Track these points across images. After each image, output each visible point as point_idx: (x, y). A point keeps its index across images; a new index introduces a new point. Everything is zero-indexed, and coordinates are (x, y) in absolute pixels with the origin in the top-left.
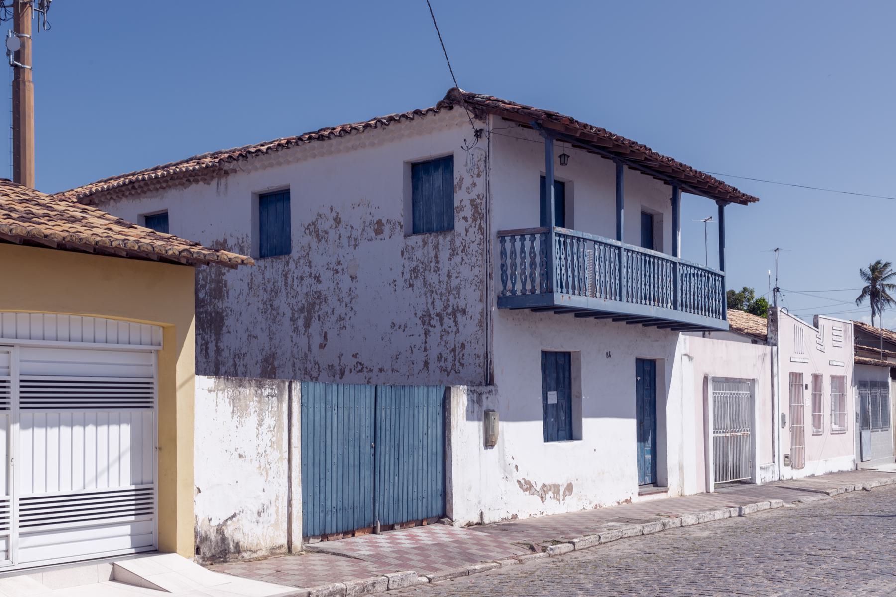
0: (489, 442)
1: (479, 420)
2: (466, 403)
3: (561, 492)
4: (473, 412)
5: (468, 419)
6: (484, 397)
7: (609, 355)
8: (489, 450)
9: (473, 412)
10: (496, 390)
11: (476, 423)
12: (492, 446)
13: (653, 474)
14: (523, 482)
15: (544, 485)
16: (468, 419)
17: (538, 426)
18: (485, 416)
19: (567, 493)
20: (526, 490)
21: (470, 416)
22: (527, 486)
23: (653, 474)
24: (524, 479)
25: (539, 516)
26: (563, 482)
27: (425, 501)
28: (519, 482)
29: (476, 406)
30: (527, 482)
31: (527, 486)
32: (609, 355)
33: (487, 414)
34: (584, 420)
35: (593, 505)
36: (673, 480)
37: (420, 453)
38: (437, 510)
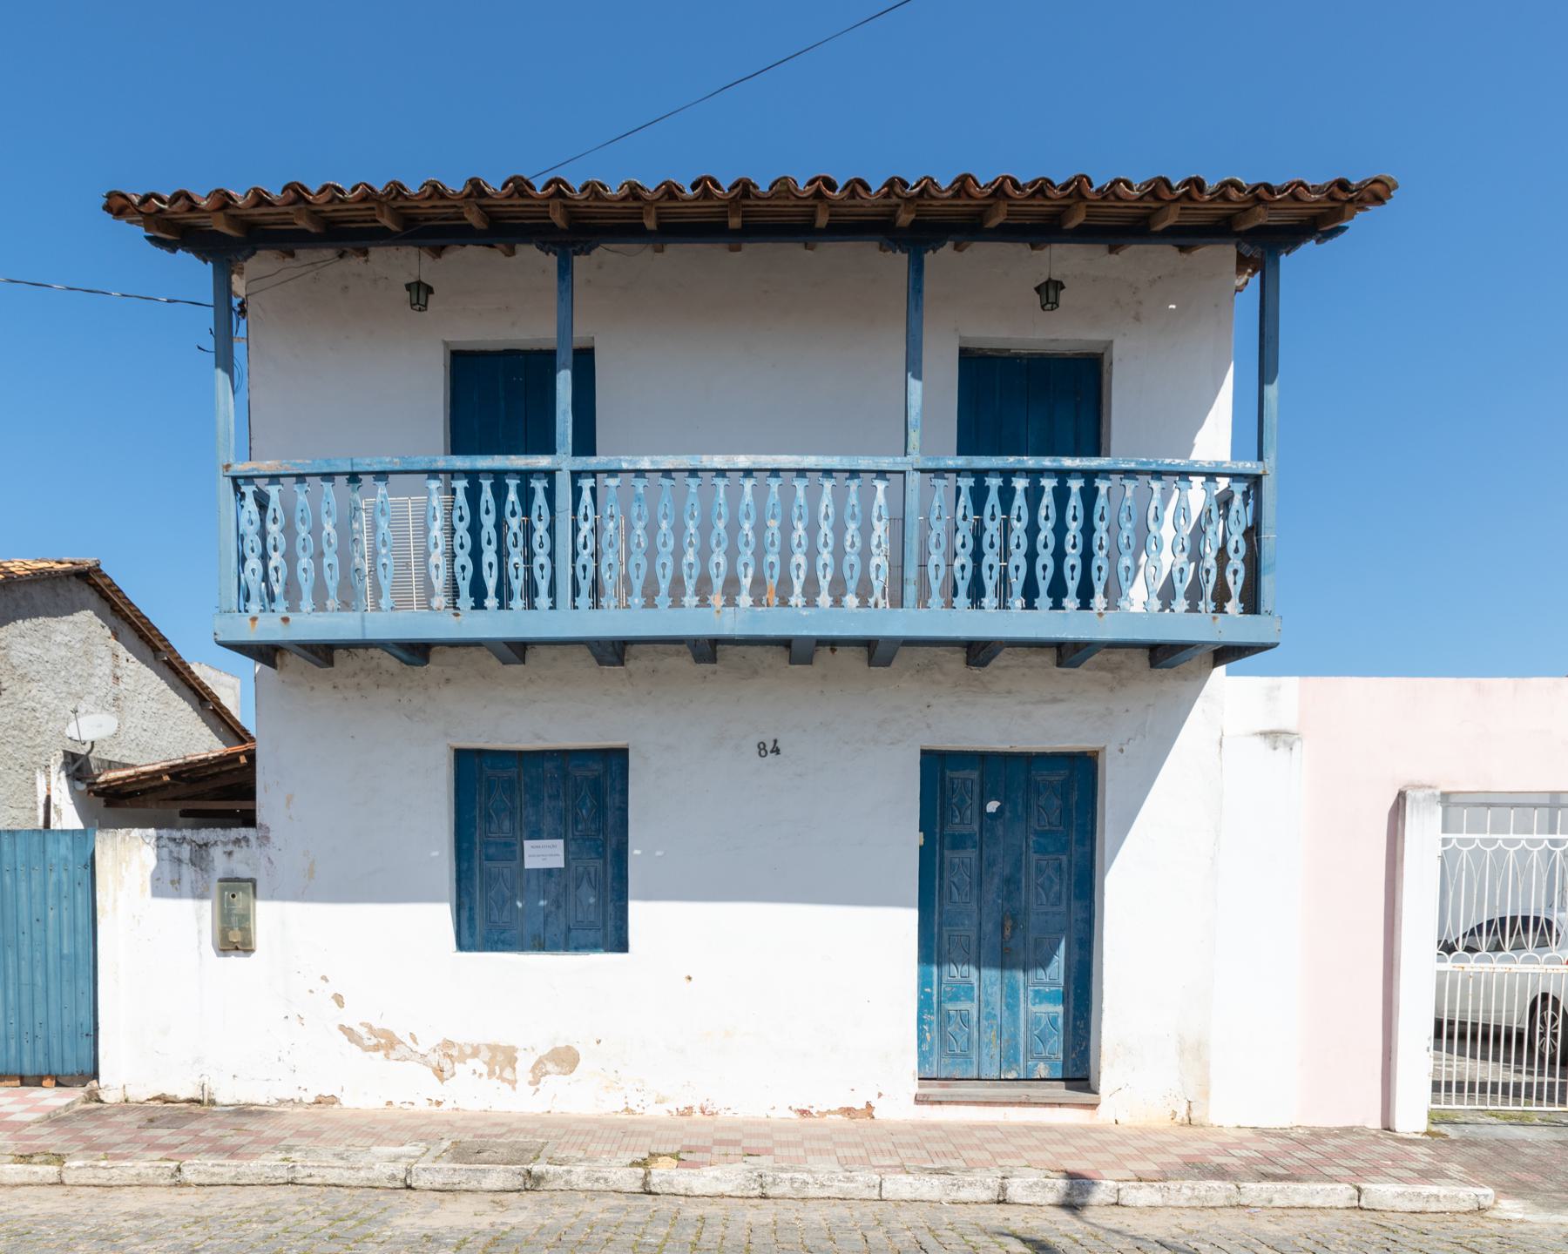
0: (234, 939)
1: (200, 896)
2: (152, 862)
3: (524, 1064)
4: (176, 882)
5: (157, 892)
6: (217, 853)
8: (235, 961)
9: (176, 882)
10: (265, 840)
11: (188, 905)
14: (363, 1032)
15: (448, 1044)
16: (157, 892)
17: (440, 917)
20: (376, 1048)
21: (165, 885)
22: (386, 1043)
24: (370, 1028)
25: (422, 1106)
26: (533, 1041)
27: (40, 1043)
29: (188, 872)
31: (386, 1043)
36: (1110, 1070)
37: (25, 952)
38: (88, 1069)
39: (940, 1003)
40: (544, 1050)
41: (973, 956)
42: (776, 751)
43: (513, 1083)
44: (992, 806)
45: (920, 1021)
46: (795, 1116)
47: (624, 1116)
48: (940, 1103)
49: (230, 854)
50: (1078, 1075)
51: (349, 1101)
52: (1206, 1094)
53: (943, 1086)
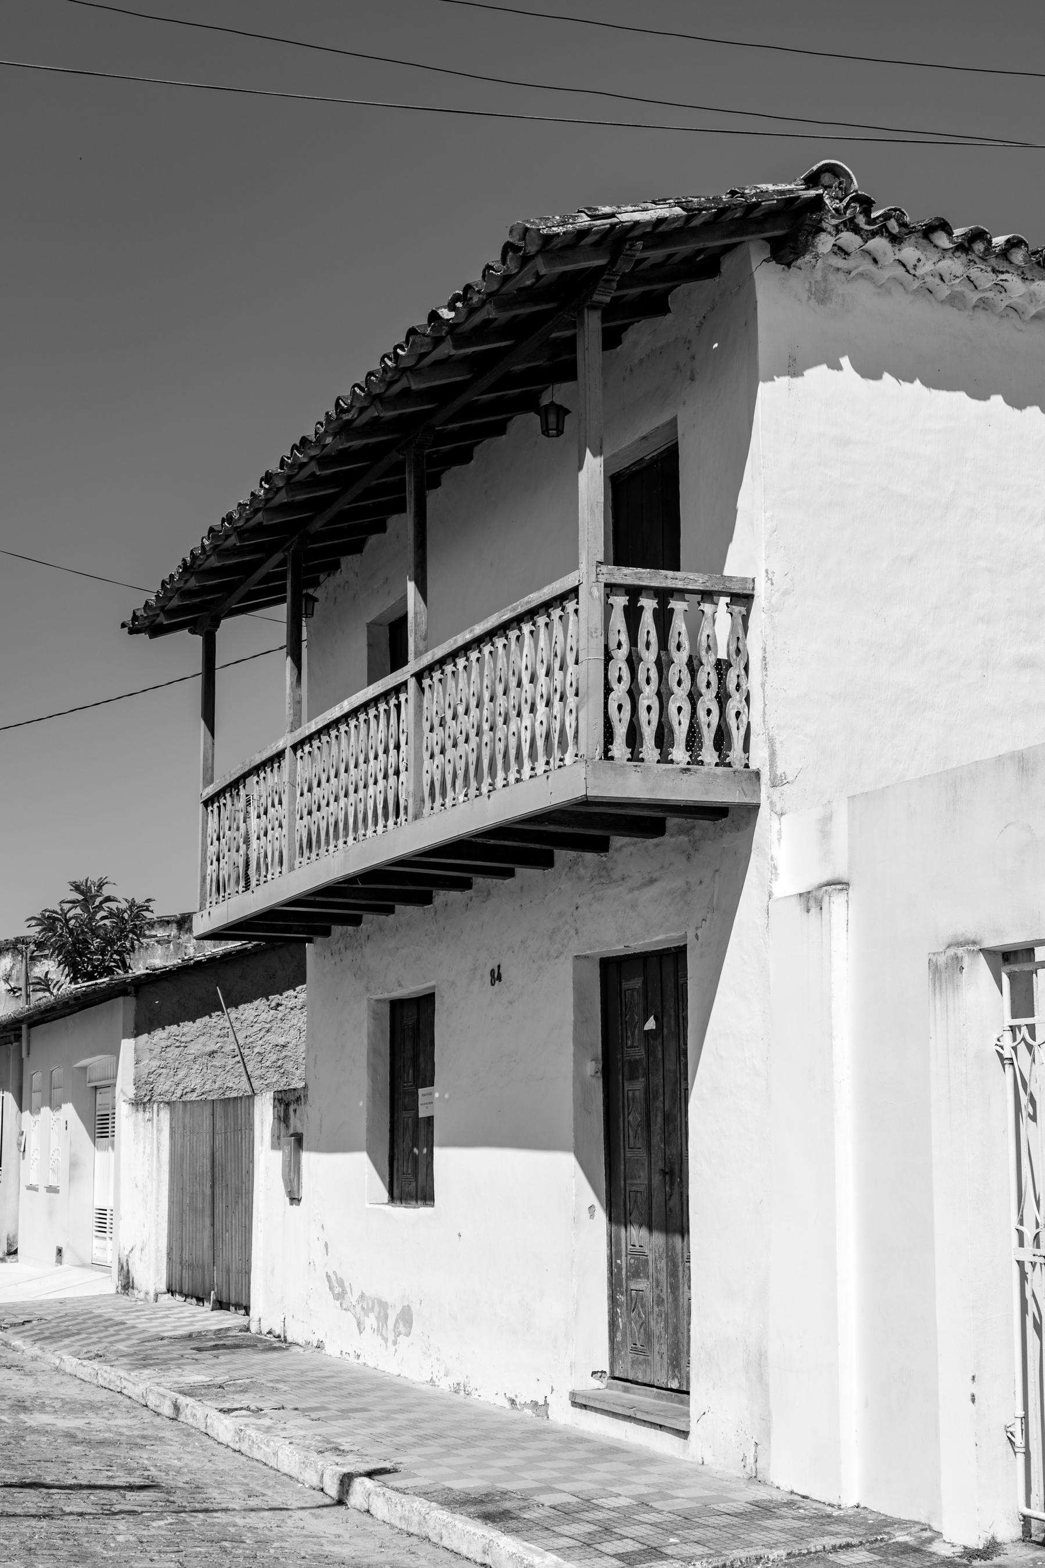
5: (273, 1147)
6: (291, 1108)
7: (496, 977)
9: (279, 1138)
12: (299, 1200)
13: (650, 1337)
18: (294, 1141)
19: (401, 1328)
23: (650, 1337)
28: (328, 1277)
29: (283, 1126)
30: (341, 1283)
32: (496, 977)
33: (299, 1140)
34: (437, 1152)
35: (452, 1380)
39: (627, 1278)
40: (399, 1309)
41: (623, 1220)
42: (499, 978)
43: (386, 1340)
44: (651, 1024)
45: (613, 1299)
46: (507, 1405)
47: (428, 1387)
48: (585, 1407)
49: (295, 1111)
50: (674, 1385)
51: (332, 1350)
52: (767, 1433)
53: (626, 1390)
